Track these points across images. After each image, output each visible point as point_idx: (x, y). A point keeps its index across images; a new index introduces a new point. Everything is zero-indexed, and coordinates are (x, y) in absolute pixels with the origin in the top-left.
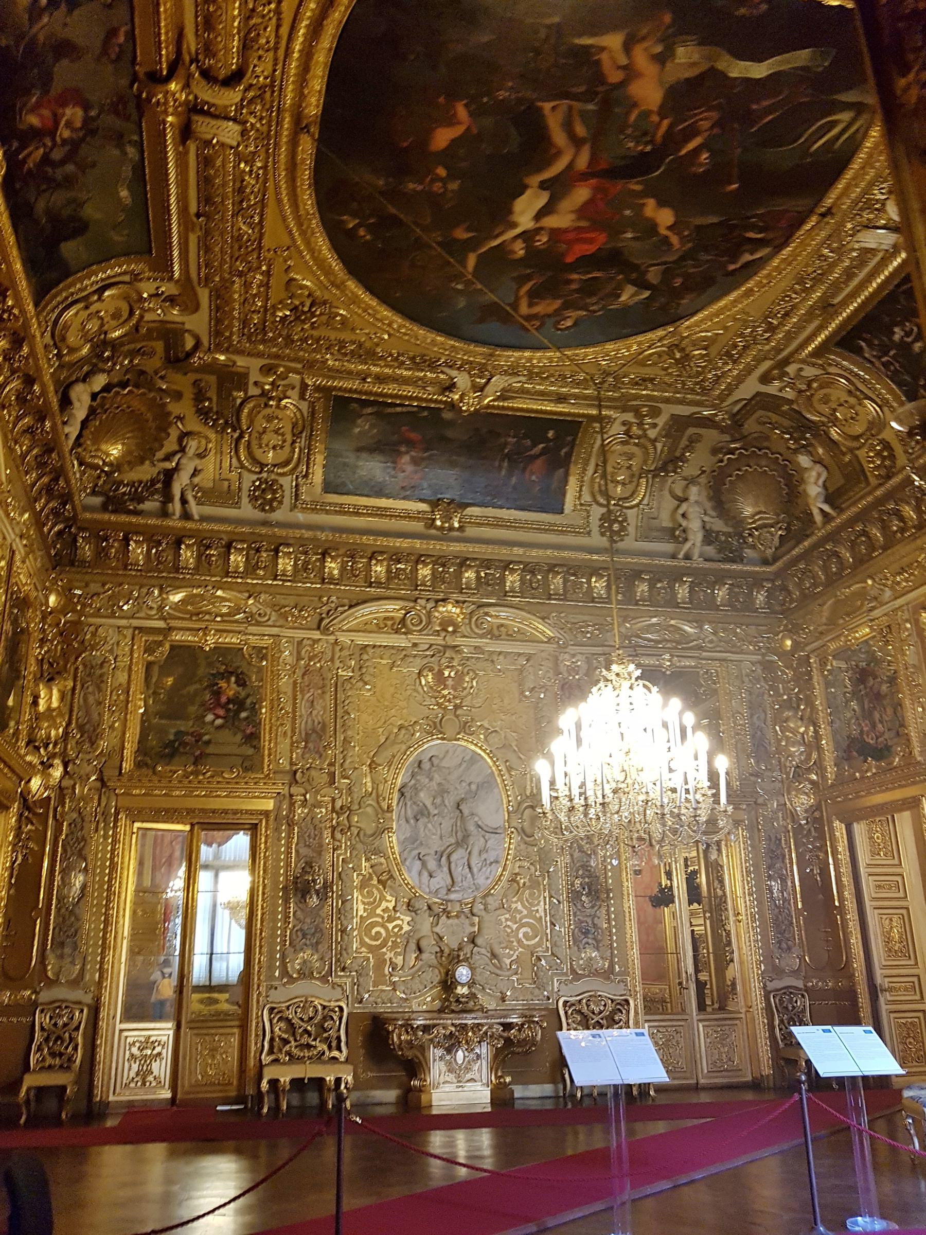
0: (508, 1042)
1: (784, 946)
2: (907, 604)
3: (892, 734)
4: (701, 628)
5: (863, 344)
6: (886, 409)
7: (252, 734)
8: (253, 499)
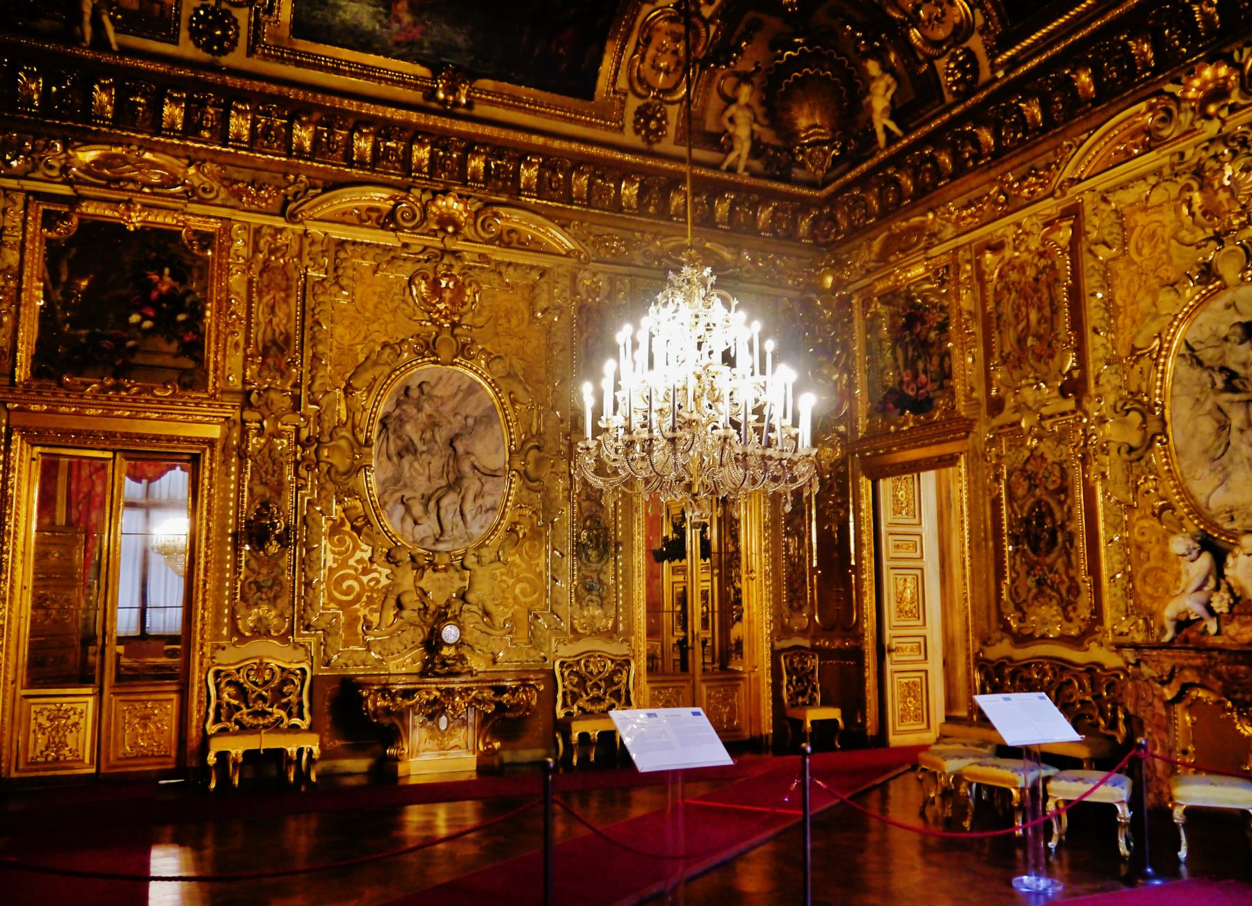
0: (500, 707)
1: (795, 605)
2: (970, 243)
3: (935, 386)
4: (739, 254)
6: (977, 11)
7: (192, 342)
8: (194, 35)
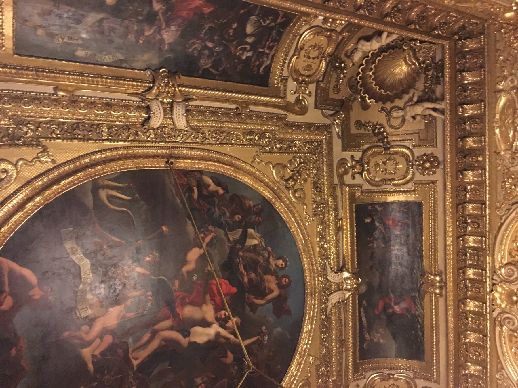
4: (500, 91)
5: (262, 69)
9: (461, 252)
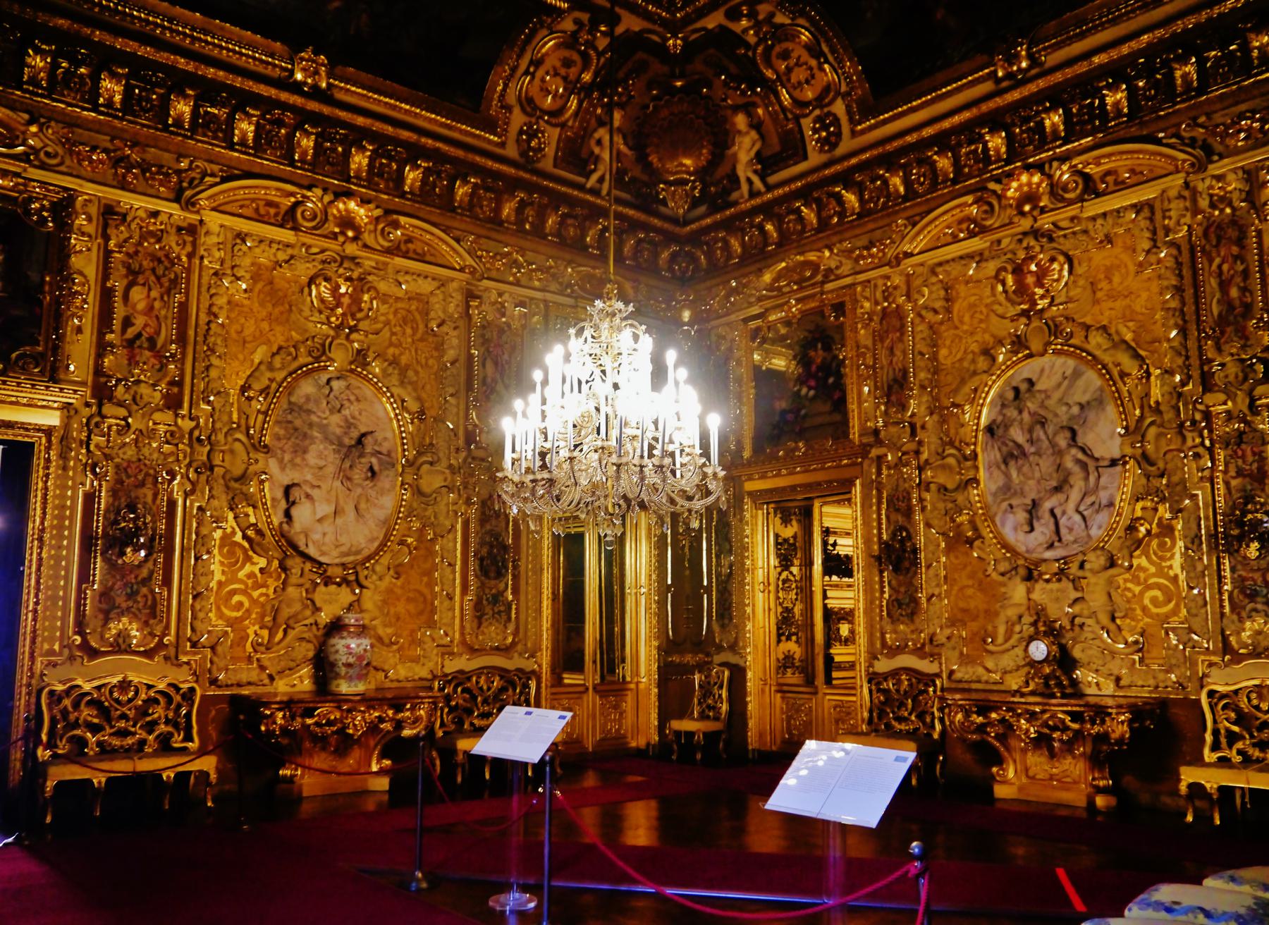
9: (1088, 86)
